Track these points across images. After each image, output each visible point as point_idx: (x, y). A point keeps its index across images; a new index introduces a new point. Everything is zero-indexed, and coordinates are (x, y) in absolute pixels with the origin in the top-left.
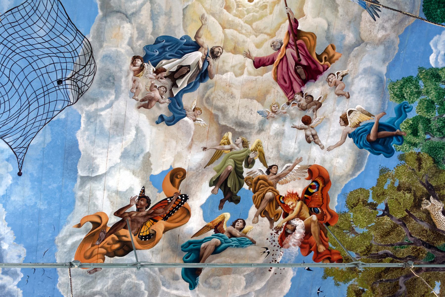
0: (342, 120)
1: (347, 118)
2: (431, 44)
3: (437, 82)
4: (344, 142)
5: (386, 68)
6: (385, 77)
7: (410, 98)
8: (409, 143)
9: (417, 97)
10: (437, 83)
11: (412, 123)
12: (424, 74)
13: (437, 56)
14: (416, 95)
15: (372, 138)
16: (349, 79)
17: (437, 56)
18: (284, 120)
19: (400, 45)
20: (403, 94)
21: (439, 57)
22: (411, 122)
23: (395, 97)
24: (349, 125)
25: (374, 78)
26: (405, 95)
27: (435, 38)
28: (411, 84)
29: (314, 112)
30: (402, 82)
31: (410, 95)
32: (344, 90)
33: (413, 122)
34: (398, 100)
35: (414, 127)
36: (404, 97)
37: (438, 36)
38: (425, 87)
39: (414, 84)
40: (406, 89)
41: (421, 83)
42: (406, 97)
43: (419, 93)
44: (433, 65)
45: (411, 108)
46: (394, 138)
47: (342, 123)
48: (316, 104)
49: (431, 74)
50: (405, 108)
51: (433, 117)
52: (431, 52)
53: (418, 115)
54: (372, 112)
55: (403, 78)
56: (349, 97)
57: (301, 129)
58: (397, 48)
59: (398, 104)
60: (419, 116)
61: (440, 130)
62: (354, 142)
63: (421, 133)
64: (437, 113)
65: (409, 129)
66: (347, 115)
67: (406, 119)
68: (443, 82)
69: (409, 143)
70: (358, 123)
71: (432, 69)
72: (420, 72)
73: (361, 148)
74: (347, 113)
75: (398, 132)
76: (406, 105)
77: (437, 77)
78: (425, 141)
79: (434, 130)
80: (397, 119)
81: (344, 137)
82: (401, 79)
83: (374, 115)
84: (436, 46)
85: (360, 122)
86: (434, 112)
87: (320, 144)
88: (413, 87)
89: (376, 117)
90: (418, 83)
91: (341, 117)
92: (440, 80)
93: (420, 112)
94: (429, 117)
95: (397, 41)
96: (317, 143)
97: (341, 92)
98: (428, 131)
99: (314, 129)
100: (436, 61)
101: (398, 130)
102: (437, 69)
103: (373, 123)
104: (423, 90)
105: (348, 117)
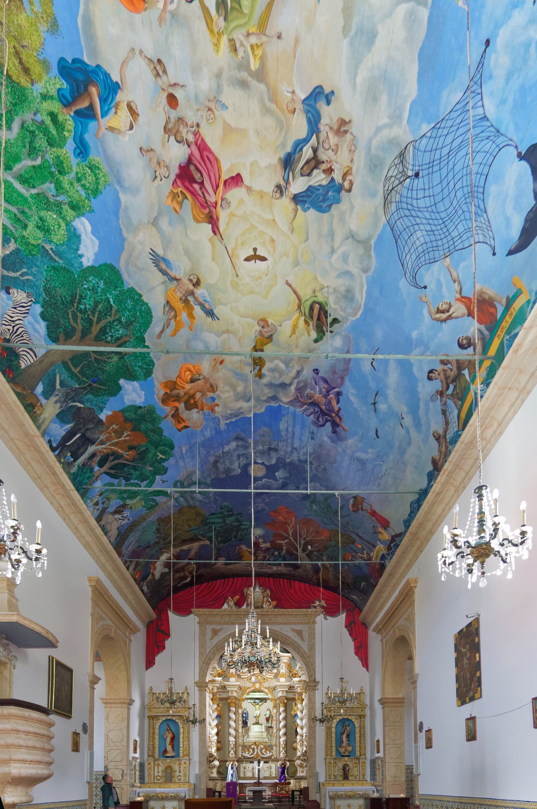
0: (136, 110)
1: (132, 115)
2: (97, 242)
3: (70, 201)
4: (120, 73)
5: (122, 200)
6: (117, 188)
7: (84, 169)
8: (52, 98)
9: (77, 173)
10: (70, 200)
11: (65, 133)
12: (86, 206)
13: (85, 231)
14: (80, 175)
15: (93, 90)
16: (149, 176)
17: (85, 231)
18: (196, 97)
19: (121, 230)
20: (91, 172)
21: (83, 230)
22: (66, 133)
23: (97, 165)
24: (125, 104)
25: (127, 184)
26: (89, 171)
27: (96, 249)
28: (91, 188)
29: (169, 118)
30: (100, 187)
31: (85, 174)
32: (148, 158)
33: (65, 135)
34: (93, 163)
35: (59, 127)
36: (89, 168)
37: (96, 251)
38: (77, 191)
39: (88, 189)
40: (93, 180)
41: (83, 193)
42: (87, 168)
43: (79, 180)
44: (83, 219)
45: (76, 155)
46: (70, 99)
47: (134, 107)
48: (169, 130)
49: (80, 208)
50: (81, 152)
51: (49, 152)
52: (93, 233)
53: (65, 148)
54: (109, 134)
55: (101, 193)
56: (141, 149)
57: (175, 84)
58: (122, 226)
59: (90, 157)
60: (63, 147)
61: (33, 136)
62: (109, 74)
63: (48, 121)
64: (49, 159)
65: (62, 122)
66: (133, 122)
67: (72, 137)
68: (66, 203)
69: (52, 98)
70: (118, 110)
71: (83, 215)
72: (90, 206)
73: (98, 66)
74: (134, 124)
75: (71, 110)
76: (82, 157)
77: (73, 206)
78: (37, 109)
79: (38, 132)
80: (81, 133)
81: (124, 81)
82: (103, 192)
83: (107, 131)
84: (92, 241)
85: (116, 113)
86: (52, 159)
87: (147, 60)
88: (88, 185)
89: (103, 129)
90: (85, 193)
91: (138, 115)
92: (69, 205)
93: (65, 154)
94: (53, 149)
95: (125, 234)
96: (150, 60)
97: (151, 154)
98: (43, 128)
99: (161, 87)
100: (83, 224)
101: (72, 114)
102: (78, 216)
103: (102, 116)
104: (76, 184)
105: (131, 118)
